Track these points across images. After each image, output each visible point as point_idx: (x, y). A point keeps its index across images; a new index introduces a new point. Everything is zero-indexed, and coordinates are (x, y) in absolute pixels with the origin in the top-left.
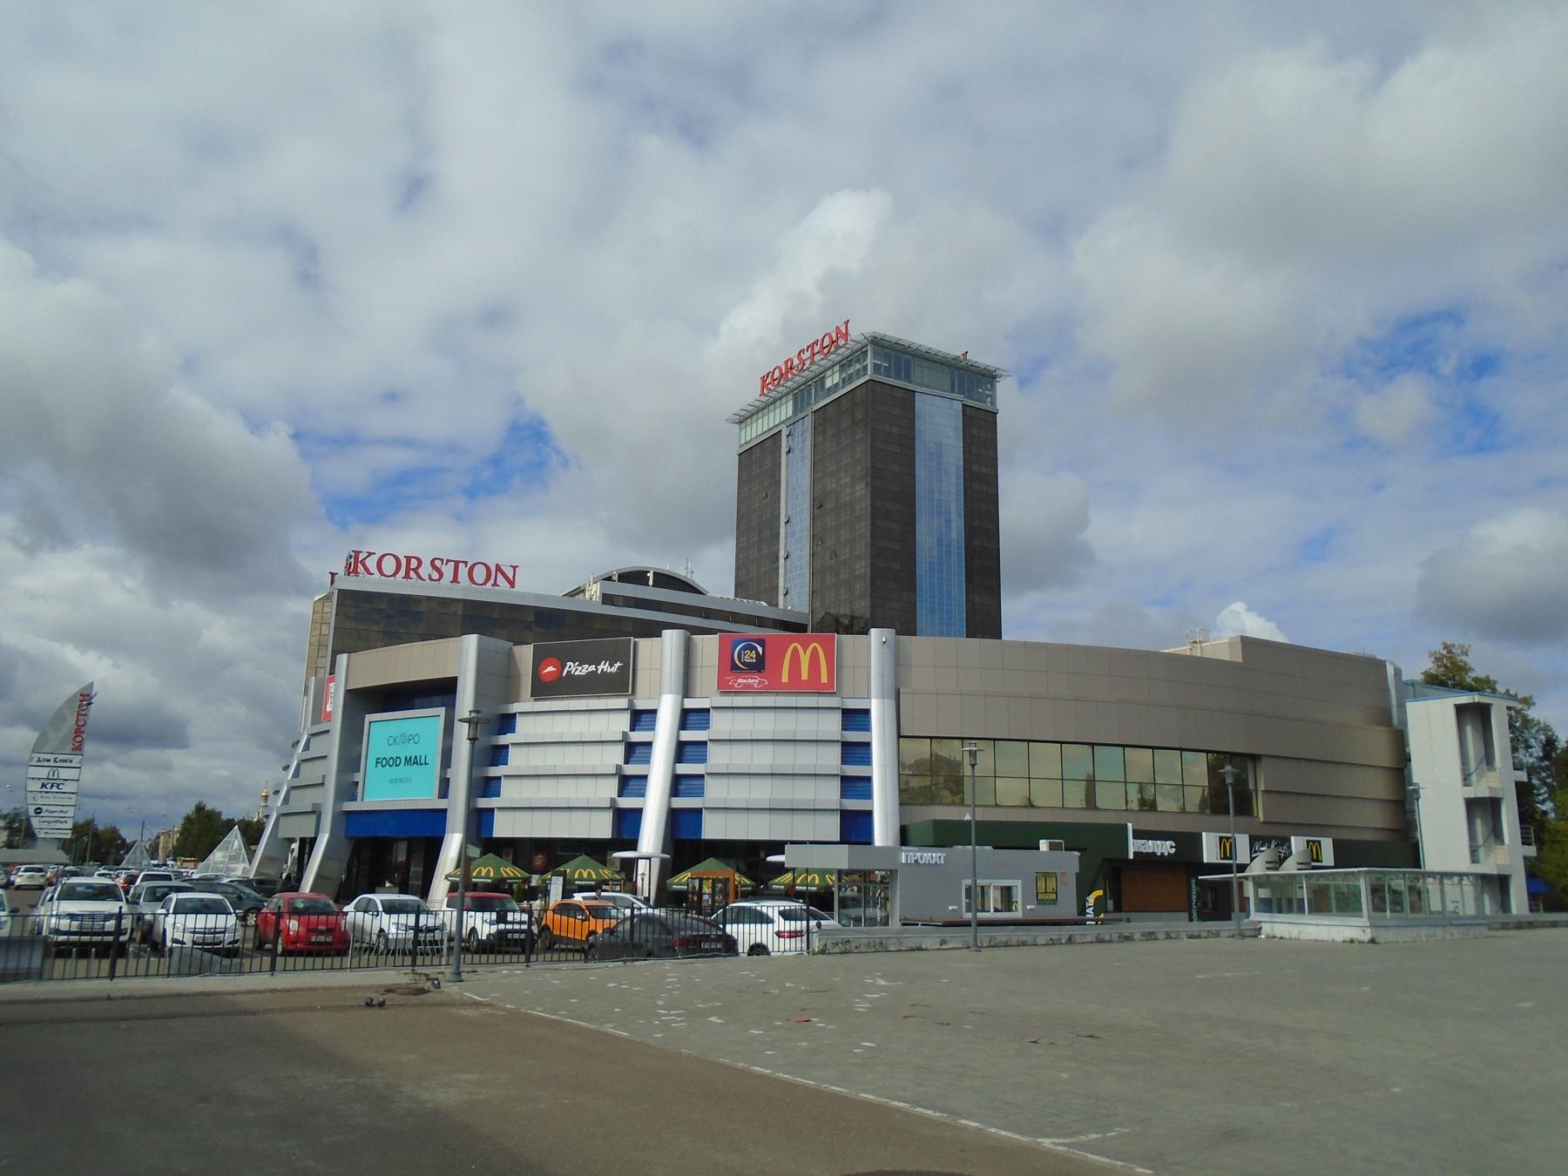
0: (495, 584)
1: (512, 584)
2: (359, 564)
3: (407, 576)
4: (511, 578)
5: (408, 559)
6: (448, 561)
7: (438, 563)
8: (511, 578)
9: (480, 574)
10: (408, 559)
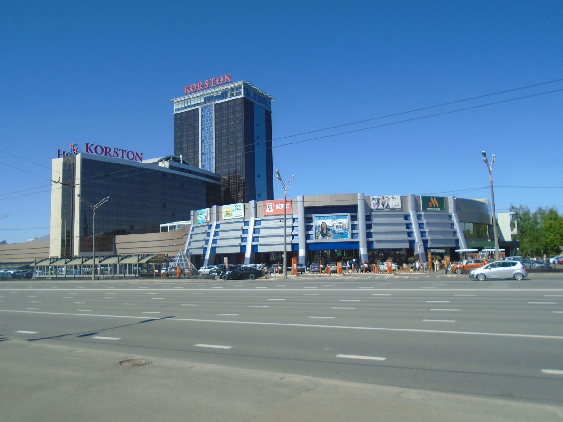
3: (106, 154)
4: (141, 158)
5: (106, 148)
6: (120, 150)
7: (116, 150)
8: (141, 158)
9: (131, 156)
10: (106, 148)
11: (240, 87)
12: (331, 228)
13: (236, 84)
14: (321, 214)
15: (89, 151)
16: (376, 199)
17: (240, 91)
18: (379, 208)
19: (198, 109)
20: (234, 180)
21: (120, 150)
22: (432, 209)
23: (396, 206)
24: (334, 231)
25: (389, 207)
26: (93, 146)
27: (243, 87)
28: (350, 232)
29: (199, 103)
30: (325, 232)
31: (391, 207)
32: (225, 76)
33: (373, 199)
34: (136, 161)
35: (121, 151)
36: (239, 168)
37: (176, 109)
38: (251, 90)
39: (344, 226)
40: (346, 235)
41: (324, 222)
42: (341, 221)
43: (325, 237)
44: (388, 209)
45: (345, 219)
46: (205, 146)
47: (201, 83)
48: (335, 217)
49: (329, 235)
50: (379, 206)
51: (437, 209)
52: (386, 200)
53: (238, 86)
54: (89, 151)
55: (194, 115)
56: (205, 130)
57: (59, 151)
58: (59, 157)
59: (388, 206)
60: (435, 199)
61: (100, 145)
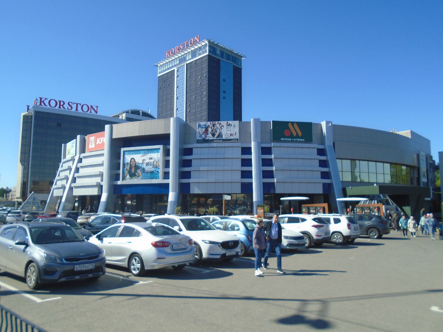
0: (91, 112)
1: (96, 112)
2: (42, 103)
3: (60, 107)
4: (96, 111)
5: (60, 102)
6: (74, 103)
7: (70, 104)
8: (96, 111)
9: (85, 108)
10: (60, 102)
12: (140, 165)
13: (203, 44)
14: (125, 148)
15: (42, 104)
16: (204, 127)
17: (206, 49)
18: (207, 138)
19: (175, 69)
21: (74, 103)
22: (290, 139)
23: (231, 135)
24: (144, 169)
25: (222, 137)
26: (46, 100)
28: (161, 171)
30: (133, 170)
31: (224, 137)
32: (195, 37)
33: (199, 126)
34: (91, 113)
35: (75, 105)
37: (159, 73)
38: (218, 49)
39: (155, 163)
40: (157, 174)
41: (133, 158)
42: (152, 157)
43: (134, 178)
44: (221, 139)
45: (157, 154)
46: (179, 103)
47: (178, 47)
48: (146, 151)
49: (137, 175)
50: (208, 136)
51: (299, 140)
52: (217, 128)
54: (42, 104)
57: (28, 106)
59: (220, 135)
60: (295, 125)
61: (55, 99)
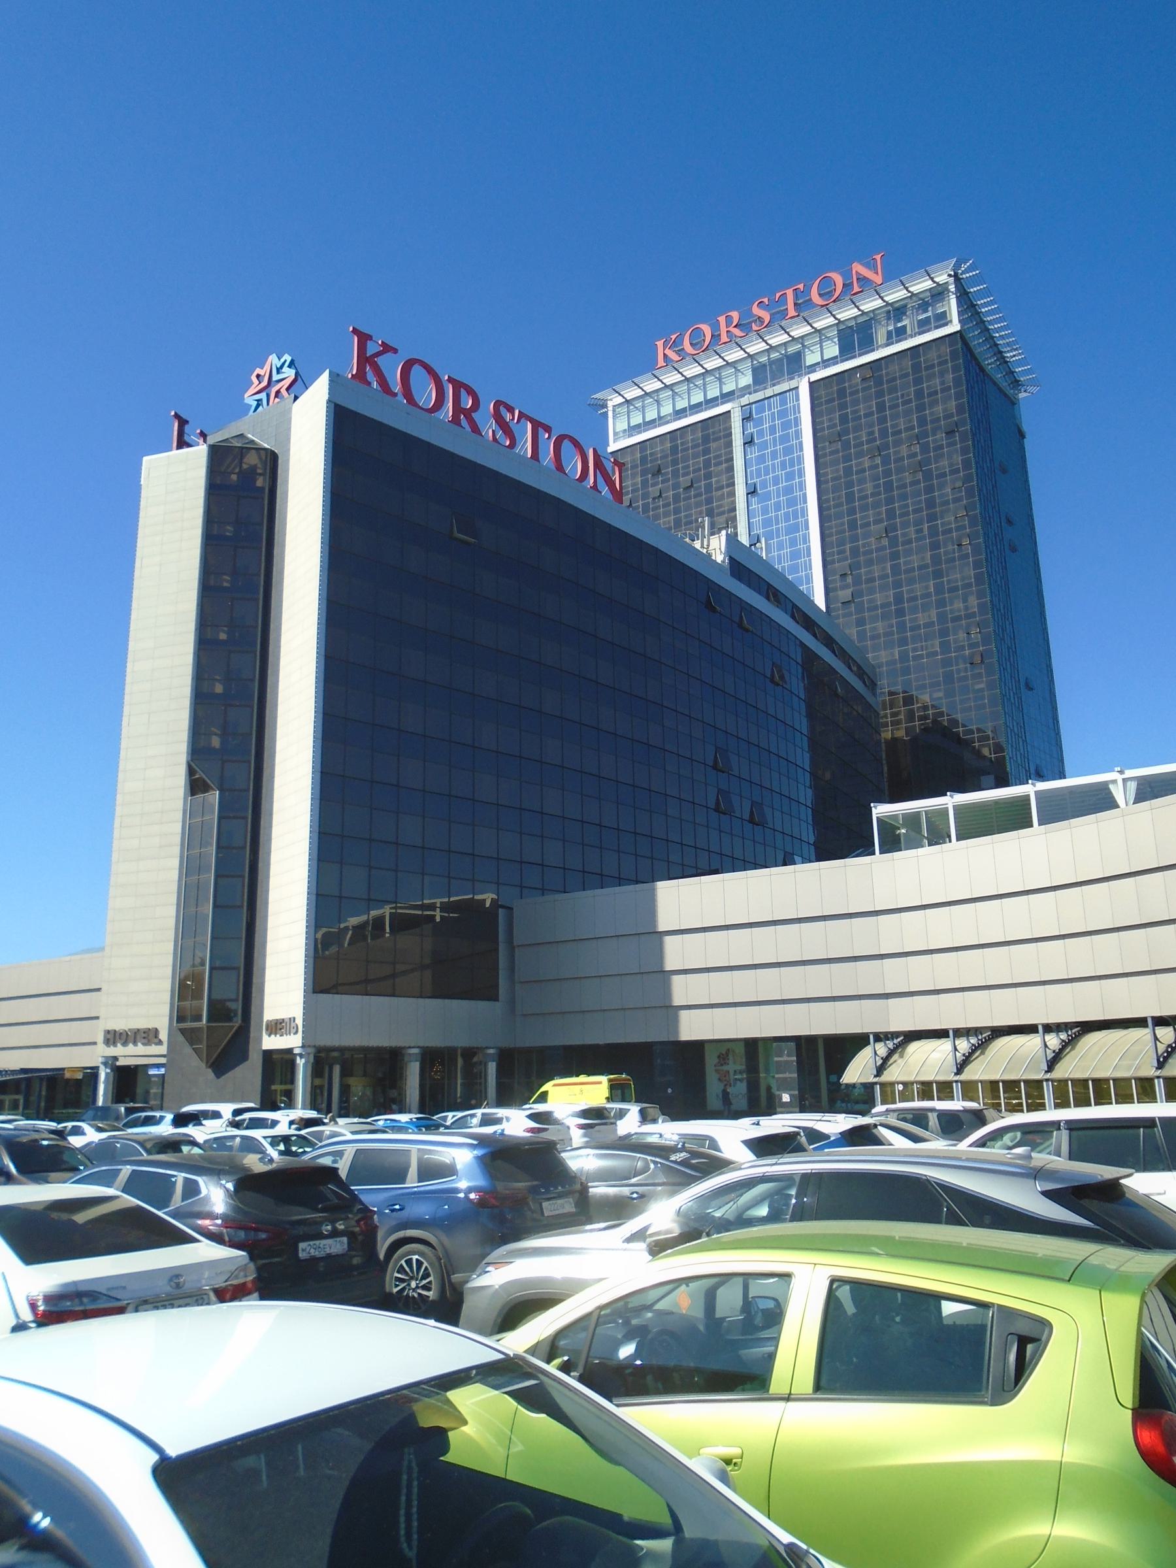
3: (455, 420)
5: (458, 385)
11: (938, 293)
13: (922, 285)
20: (936, 695)
27: (952, 288)
29: (732, 393)
36: (962, 635)
37: (615, 434)
47: (735, 315)
53: (928, 294)
55: (706, 439)
56: (767, 497)
58: (182, 444)
